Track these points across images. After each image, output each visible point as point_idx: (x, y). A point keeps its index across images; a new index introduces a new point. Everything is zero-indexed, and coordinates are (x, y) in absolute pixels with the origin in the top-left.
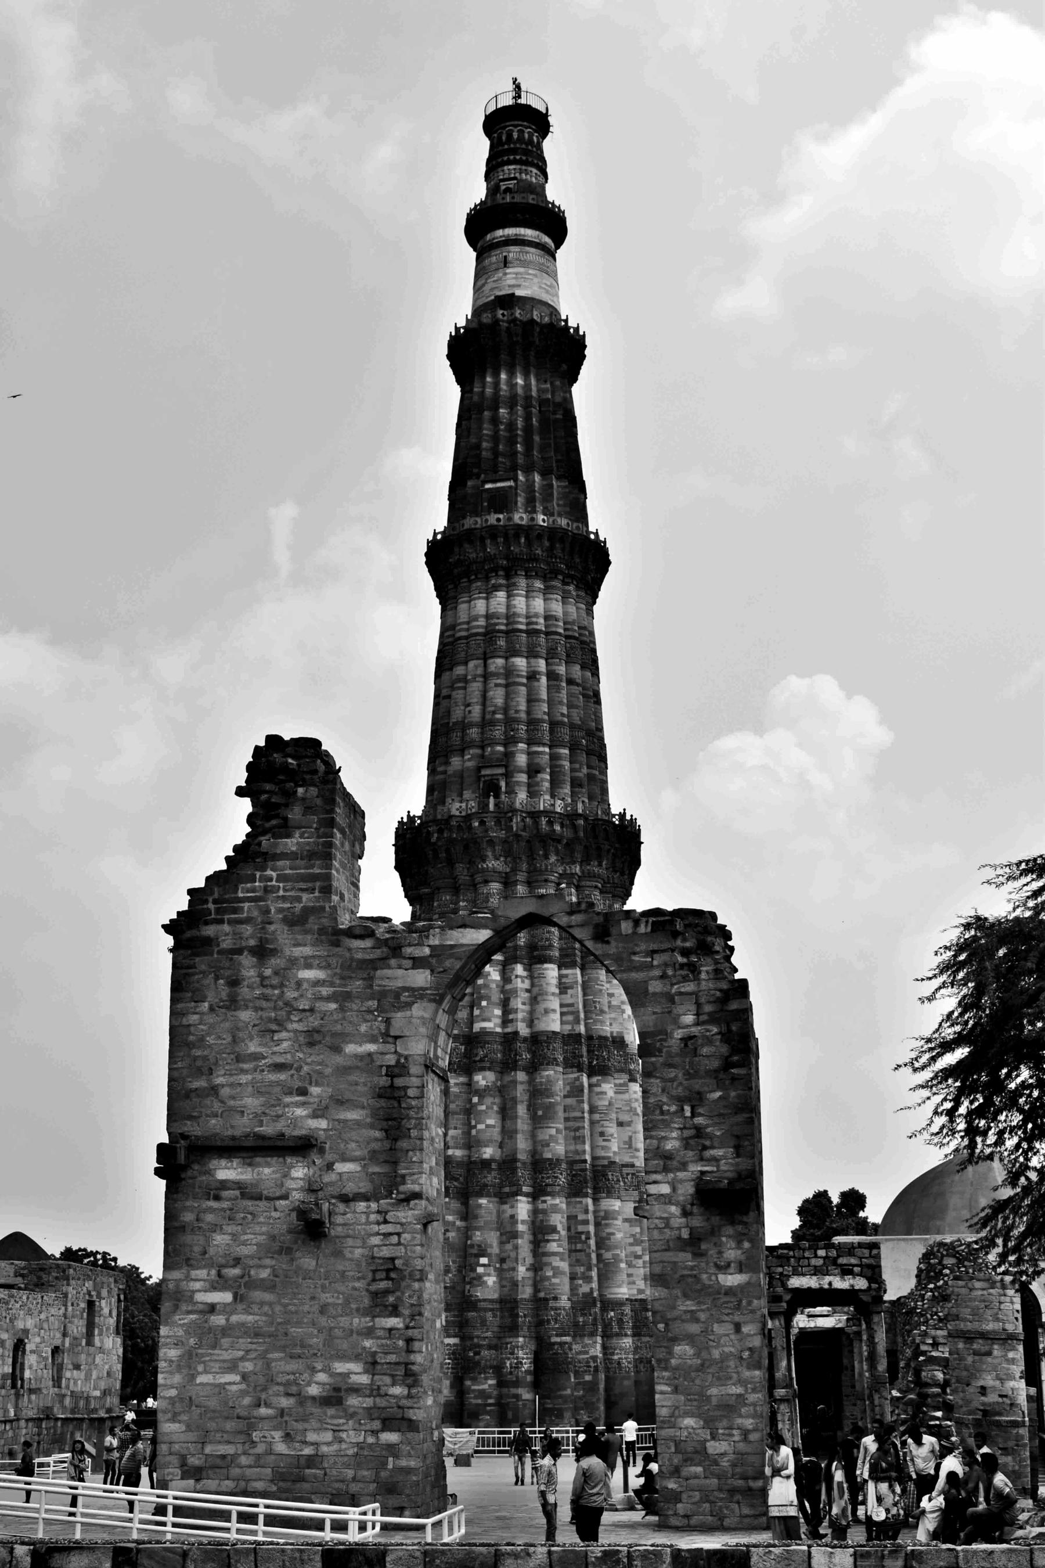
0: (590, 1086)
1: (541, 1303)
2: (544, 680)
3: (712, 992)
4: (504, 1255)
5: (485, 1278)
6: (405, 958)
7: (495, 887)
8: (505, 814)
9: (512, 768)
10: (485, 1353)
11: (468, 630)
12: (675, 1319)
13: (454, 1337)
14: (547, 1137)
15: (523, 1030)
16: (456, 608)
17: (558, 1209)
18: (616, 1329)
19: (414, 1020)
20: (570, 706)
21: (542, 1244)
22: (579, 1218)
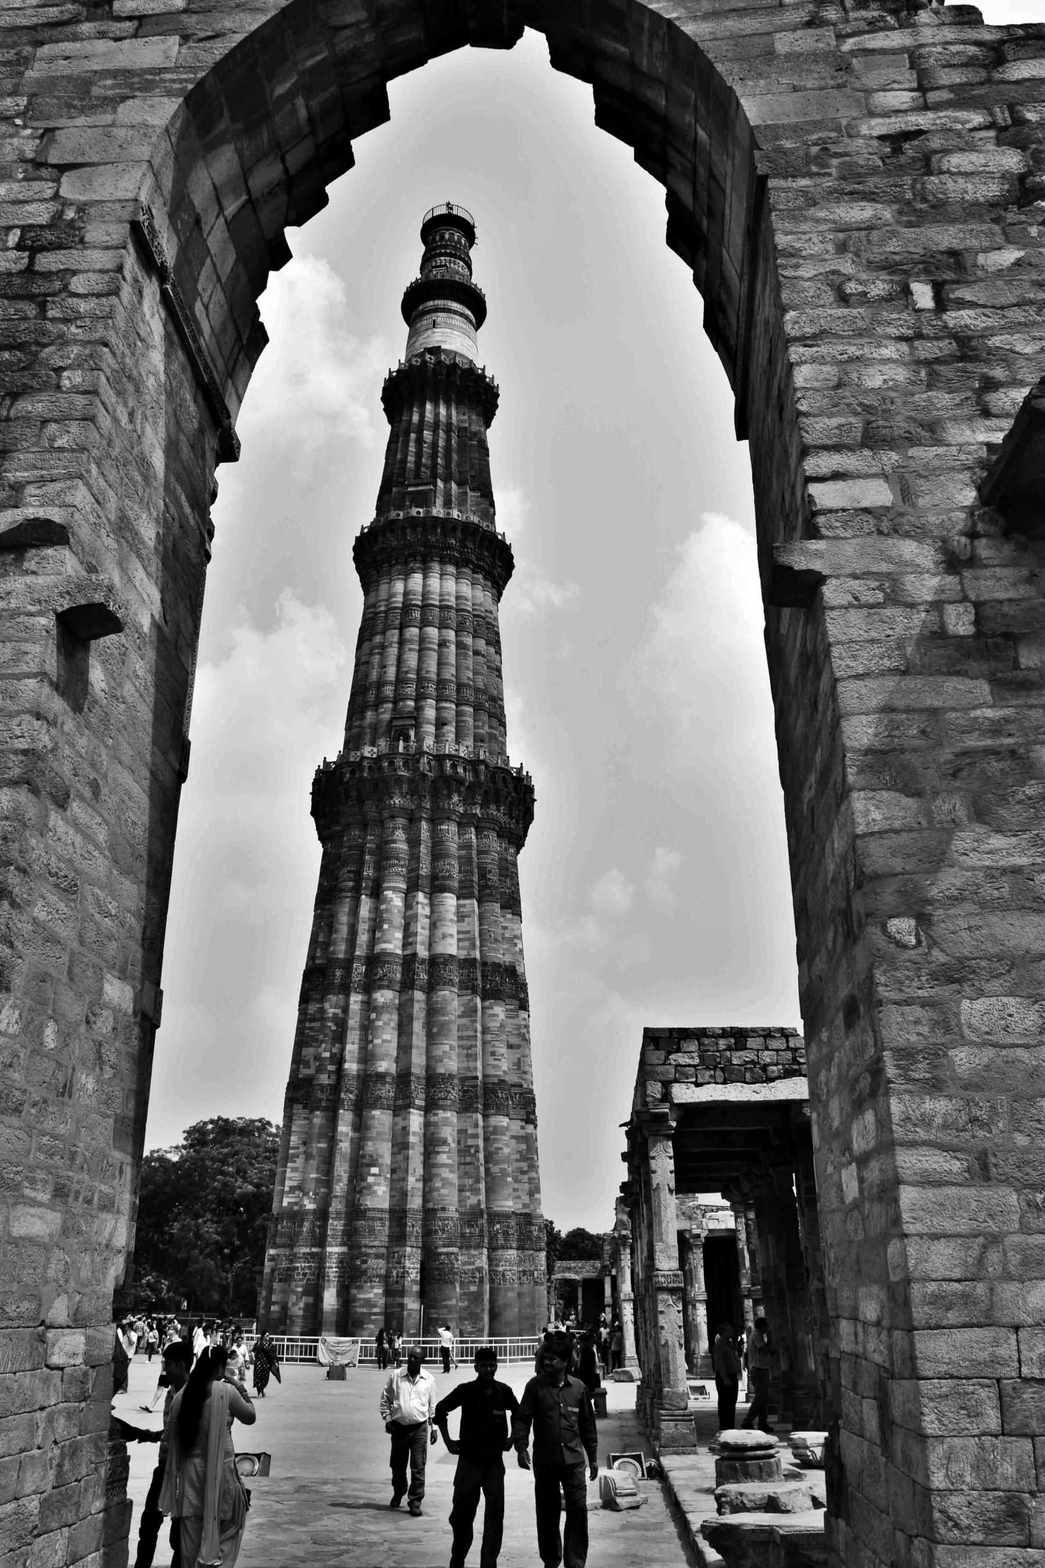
0: (483, 1008)
1: (429, 1213)
2: (453, 647)
3: (954, 48)
6: (119, 19)
7: (401, 821)
8: (412, 760)
10: (372, 1262)
12: (957, 900)
13: (341, 1245)
15: (423, 952)
17: (449, 1123)
18: (501, 1242)
19: (120, 133)
20: (475, 673)
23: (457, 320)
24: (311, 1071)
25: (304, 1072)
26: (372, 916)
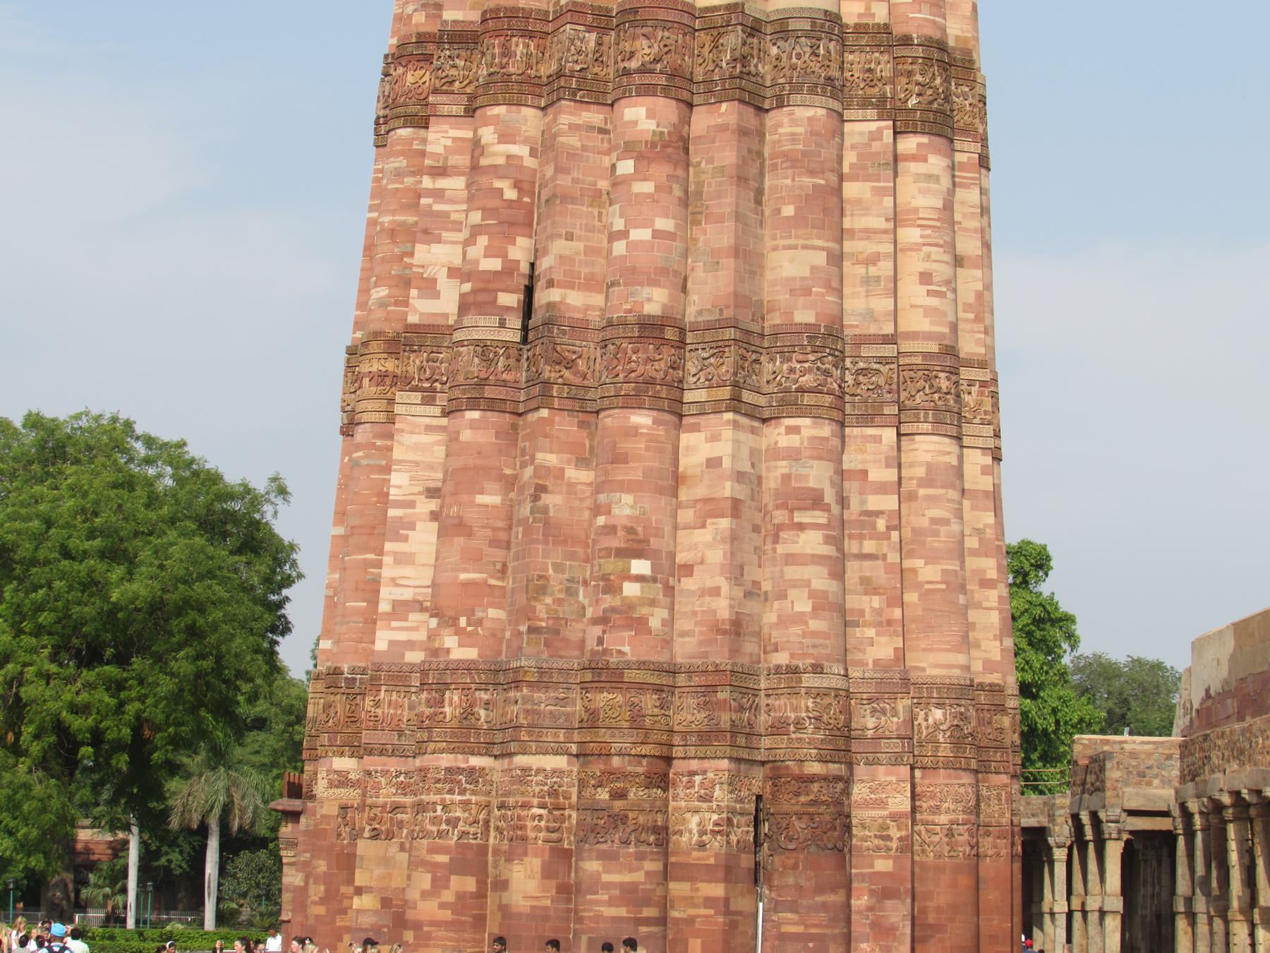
4: (681, 558)
5: (645, 611)
14: (807, 273)
24: (445, 303)
25: (420, 309)
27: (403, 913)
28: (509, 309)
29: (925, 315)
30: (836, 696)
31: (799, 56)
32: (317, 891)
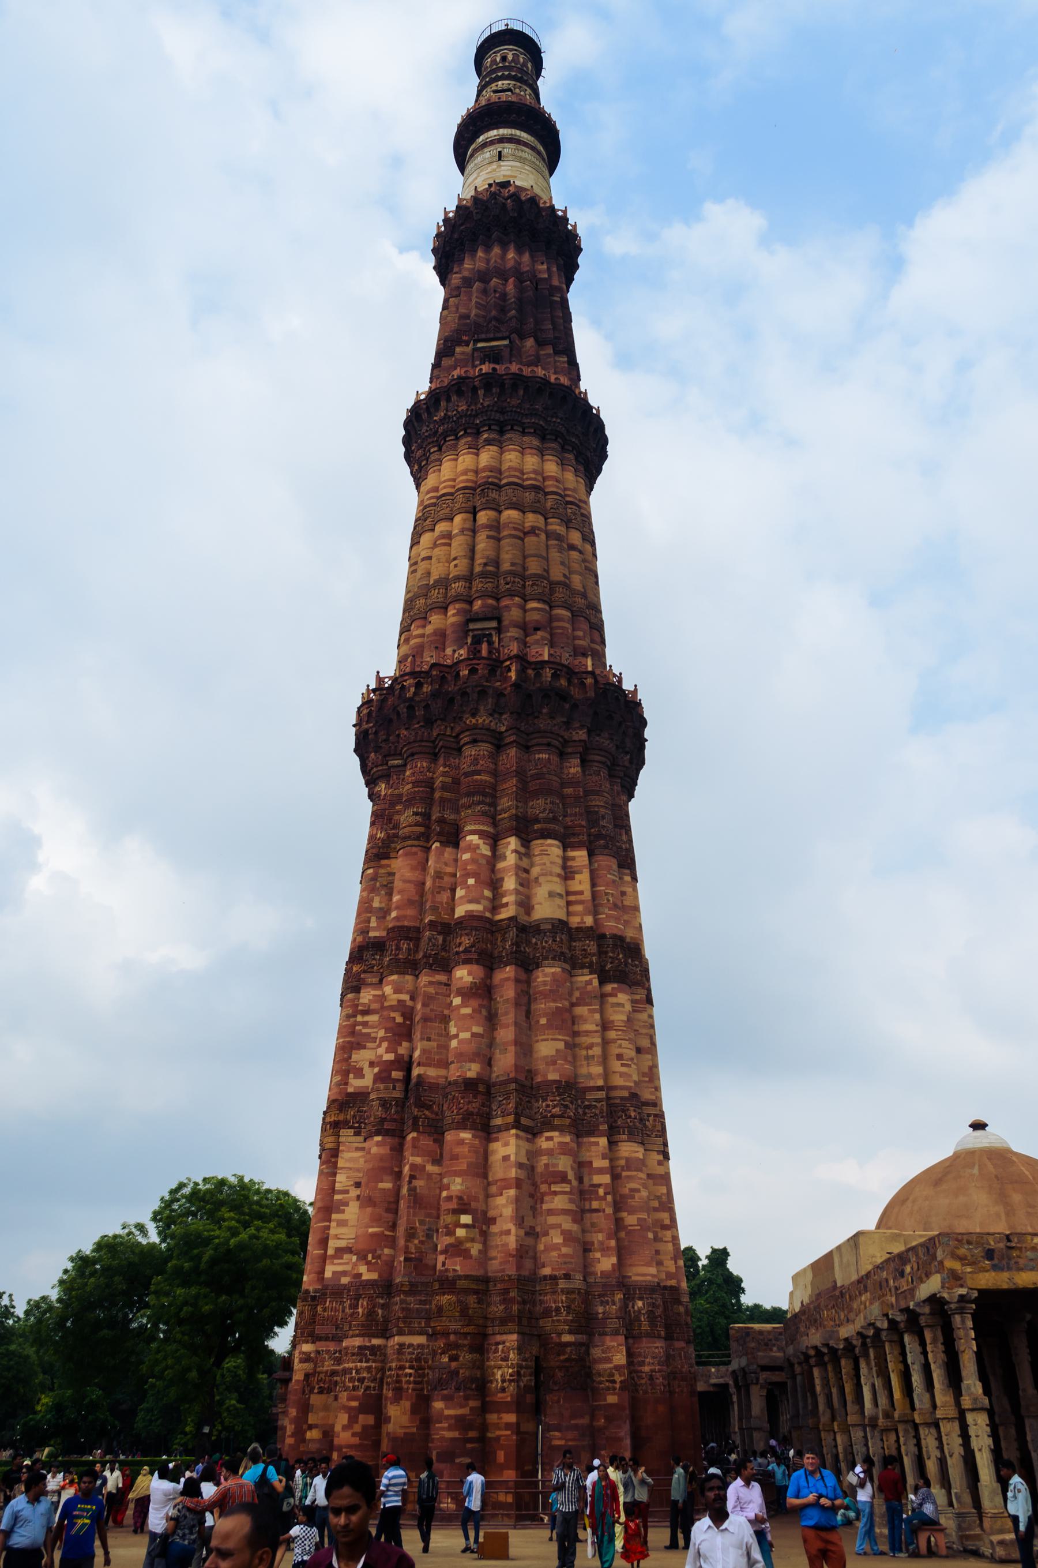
2: (543, 536)
4: (491, 1213)
5: (468, 1245)
9: (505, 623)
11: (454, 487)
13: (420, 1334)
14: (554, 1053)
15: (523, 919)
16: (440, 470)
21: (546, 1198)
22: (595, 1165)
23: (527, 154)
24: (367, 1081)
25: (355, 1084)
26: (449, 870)
27: (332, 1440)
28: (398, 1080)
29: (621, 1076)
30: (579, 1293)
31: (546, 942)
32: (290, 1429)
